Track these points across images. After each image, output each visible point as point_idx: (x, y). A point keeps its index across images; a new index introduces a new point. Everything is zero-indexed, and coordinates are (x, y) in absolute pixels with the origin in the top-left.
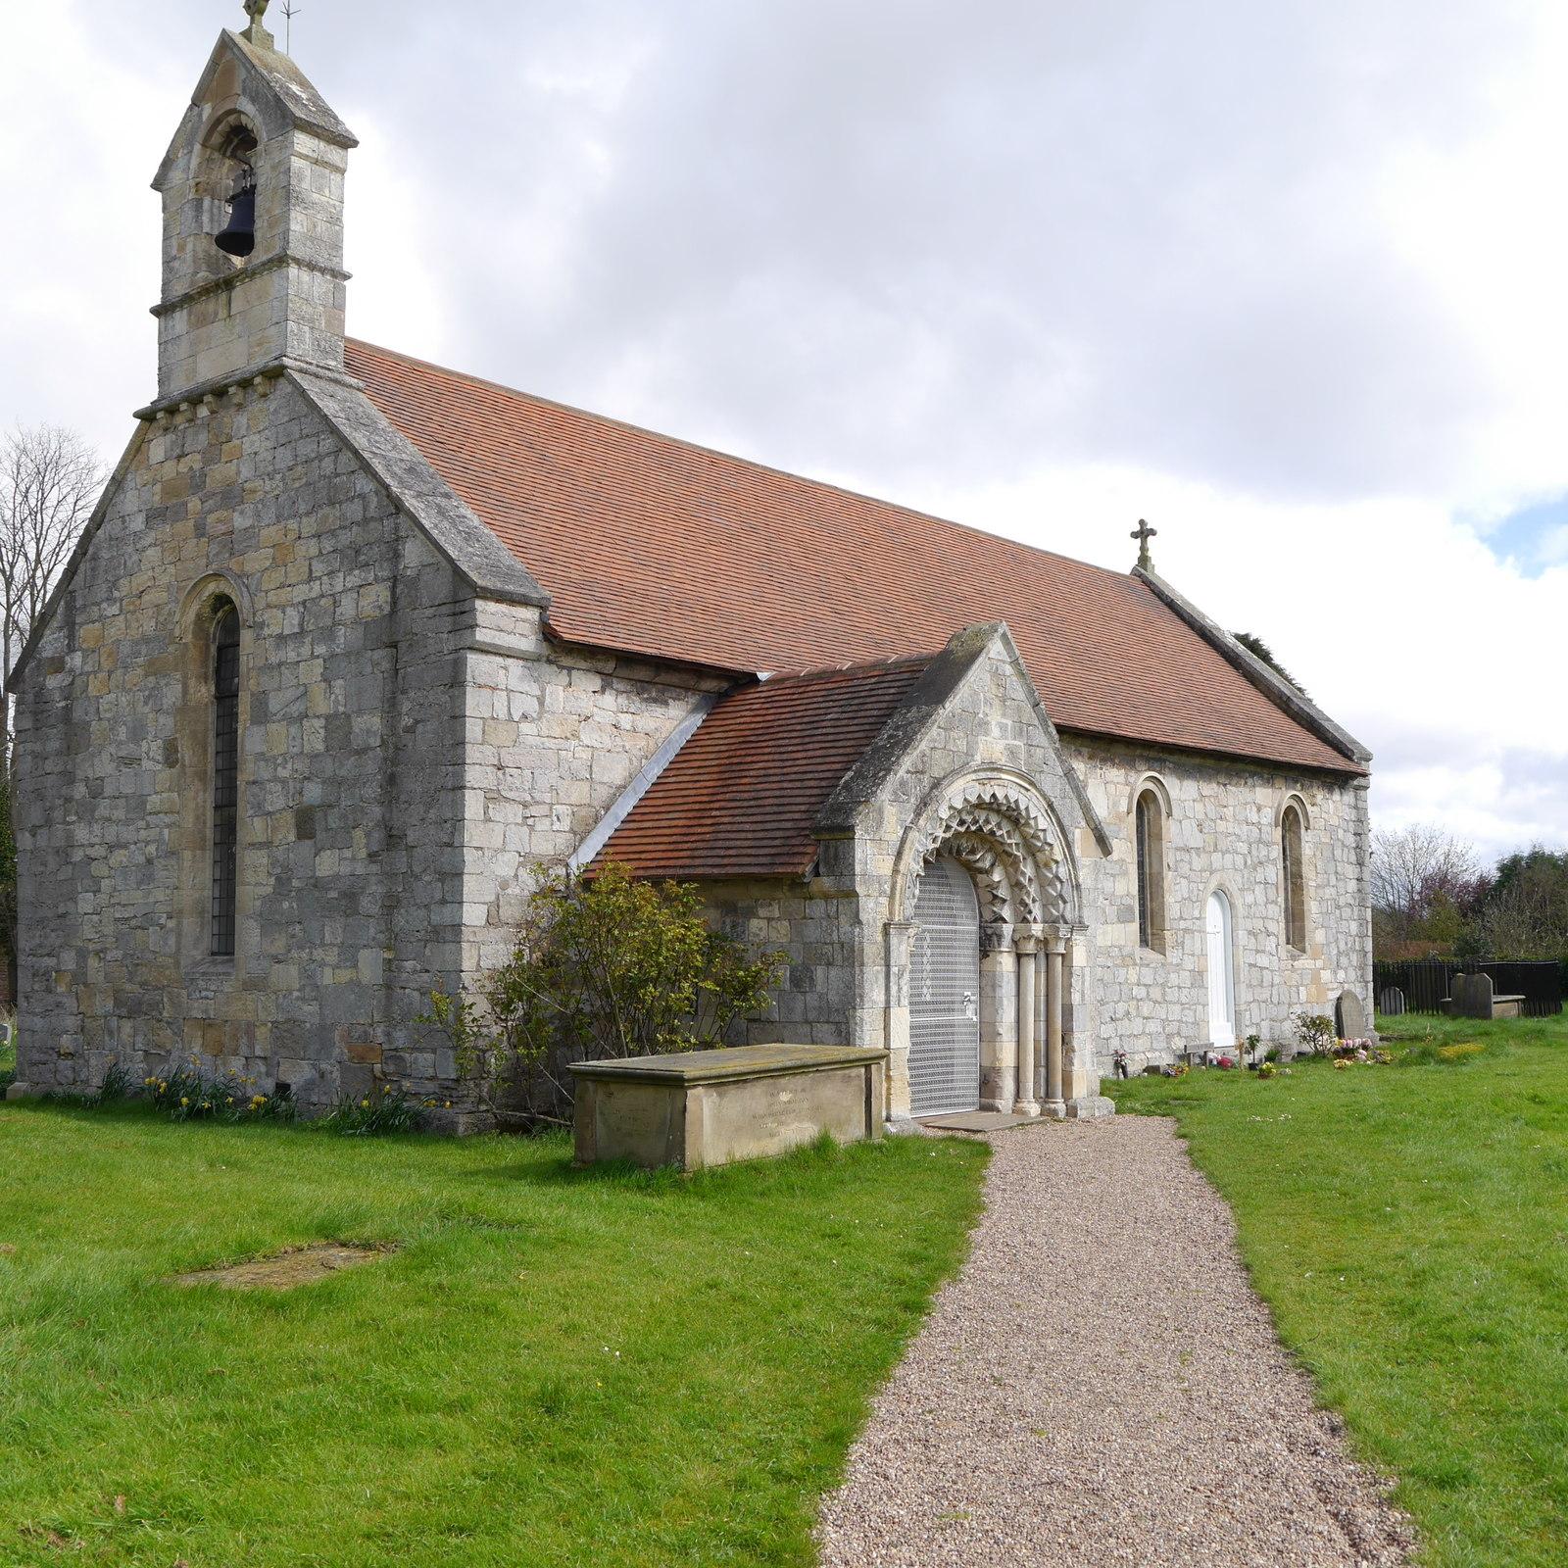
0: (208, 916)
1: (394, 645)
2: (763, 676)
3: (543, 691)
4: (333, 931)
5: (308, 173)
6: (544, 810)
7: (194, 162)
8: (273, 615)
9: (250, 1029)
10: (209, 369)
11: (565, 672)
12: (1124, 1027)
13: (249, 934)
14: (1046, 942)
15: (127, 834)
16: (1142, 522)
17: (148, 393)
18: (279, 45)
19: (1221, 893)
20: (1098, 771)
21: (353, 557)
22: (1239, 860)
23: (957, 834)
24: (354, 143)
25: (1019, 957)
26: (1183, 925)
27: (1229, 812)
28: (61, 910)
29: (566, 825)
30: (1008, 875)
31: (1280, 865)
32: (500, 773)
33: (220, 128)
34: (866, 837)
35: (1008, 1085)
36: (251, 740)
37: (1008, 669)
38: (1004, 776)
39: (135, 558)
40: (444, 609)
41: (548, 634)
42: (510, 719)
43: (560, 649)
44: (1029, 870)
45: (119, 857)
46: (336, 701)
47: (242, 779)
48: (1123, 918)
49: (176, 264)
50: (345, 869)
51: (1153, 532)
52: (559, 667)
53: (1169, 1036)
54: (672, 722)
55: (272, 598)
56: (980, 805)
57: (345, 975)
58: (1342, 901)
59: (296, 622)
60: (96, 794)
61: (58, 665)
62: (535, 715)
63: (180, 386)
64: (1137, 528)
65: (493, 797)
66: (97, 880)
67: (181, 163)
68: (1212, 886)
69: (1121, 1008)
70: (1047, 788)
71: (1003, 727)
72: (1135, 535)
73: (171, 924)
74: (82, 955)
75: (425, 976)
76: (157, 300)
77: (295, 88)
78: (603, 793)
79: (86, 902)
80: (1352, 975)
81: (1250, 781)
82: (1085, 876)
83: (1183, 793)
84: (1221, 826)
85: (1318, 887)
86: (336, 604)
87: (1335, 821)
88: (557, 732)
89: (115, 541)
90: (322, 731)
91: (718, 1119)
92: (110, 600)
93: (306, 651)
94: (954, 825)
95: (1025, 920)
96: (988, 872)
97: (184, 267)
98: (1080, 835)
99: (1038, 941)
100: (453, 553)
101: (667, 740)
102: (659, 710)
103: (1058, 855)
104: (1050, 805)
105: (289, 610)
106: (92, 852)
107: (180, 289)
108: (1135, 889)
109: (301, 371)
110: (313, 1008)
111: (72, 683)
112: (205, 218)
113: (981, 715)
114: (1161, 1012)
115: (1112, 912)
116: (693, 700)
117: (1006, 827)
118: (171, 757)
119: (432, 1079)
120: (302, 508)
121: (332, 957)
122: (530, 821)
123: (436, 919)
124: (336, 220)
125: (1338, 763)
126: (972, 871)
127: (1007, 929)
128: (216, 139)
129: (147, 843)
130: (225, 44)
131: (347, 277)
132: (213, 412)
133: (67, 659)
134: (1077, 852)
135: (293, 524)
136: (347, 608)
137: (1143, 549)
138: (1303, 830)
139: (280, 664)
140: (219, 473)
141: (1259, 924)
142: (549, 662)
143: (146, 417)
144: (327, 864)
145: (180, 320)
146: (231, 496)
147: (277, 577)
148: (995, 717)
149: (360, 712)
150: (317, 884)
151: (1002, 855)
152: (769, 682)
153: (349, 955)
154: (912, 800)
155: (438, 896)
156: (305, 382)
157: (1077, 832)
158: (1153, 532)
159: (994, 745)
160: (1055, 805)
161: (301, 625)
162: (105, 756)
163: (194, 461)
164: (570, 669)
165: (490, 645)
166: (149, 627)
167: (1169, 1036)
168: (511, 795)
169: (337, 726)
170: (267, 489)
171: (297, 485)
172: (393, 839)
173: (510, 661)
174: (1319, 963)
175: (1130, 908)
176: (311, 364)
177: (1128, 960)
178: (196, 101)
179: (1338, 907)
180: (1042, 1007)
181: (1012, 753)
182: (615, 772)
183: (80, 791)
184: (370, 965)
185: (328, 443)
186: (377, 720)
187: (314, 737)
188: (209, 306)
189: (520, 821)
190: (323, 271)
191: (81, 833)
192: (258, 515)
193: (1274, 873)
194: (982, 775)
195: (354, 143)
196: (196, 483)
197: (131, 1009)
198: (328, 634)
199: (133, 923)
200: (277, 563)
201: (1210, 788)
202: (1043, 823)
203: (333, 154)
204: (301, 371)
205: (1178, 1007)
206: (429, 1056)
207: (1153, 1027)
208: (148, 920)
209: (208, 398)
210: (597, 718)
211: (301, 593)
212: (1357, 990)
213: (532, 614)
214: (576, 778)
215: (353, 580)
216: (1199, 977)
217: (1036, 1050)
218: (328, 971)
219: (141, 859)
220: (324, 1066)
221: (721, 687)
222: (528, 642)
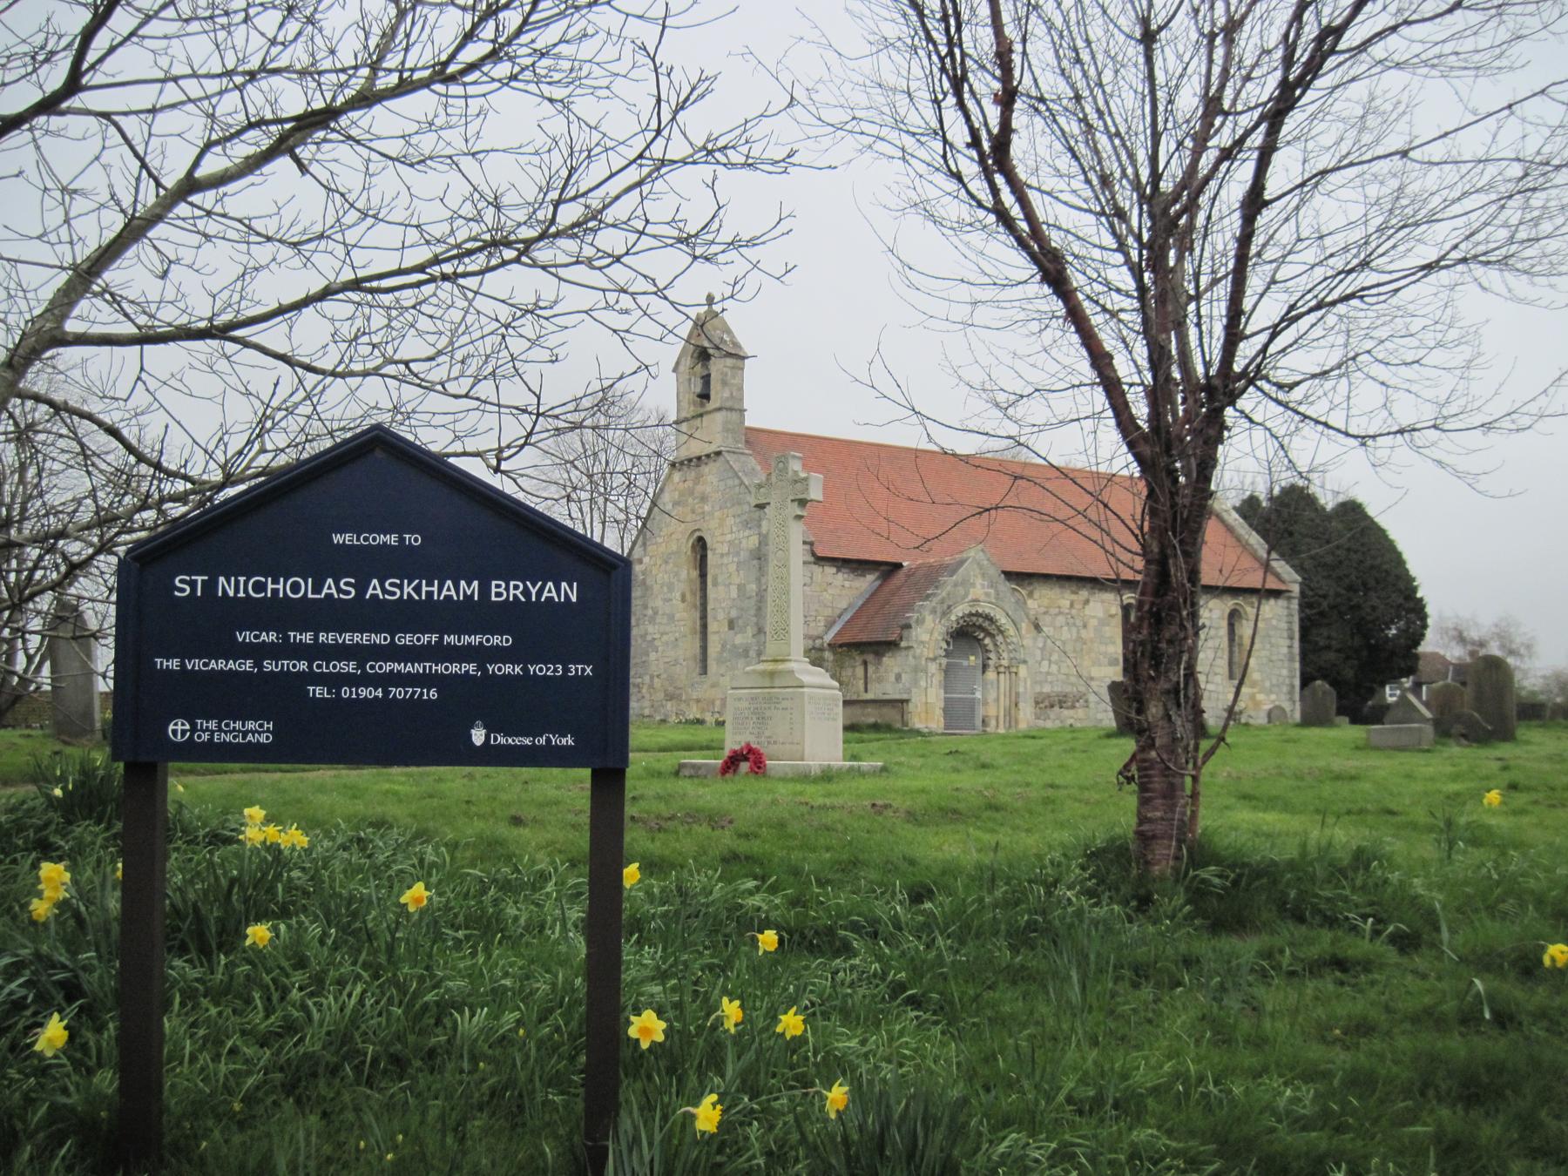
9: (713, 703)
13: (712, 666)
15: (668, 629)
21: (746, 524)
35: (993, 723)
44: (1000, 638)
45: (665, 638)
54: (869, 581)
56: (971, 614)
60: (656, 613)
74: (652, 677)
79: (653, 656)
80: (1283, 697)
82: (1027, 642)
97: (685, 404)
107: (684, 415)
118: (683, 600)
124: (741, 389)
136: (744, 544)
140: (699, 488)
144: (739, 639)
146: (704, 499)
148: (979, 581)
150: (734, 646)
151: (988, 634)
163: (689, 484)
166: (674, 548)
169: (741, 588)
175: (1117, 659)
181: (987, 595)
182: (844, 605)
183: (650, 612)
185: (737, 482)
186: (754, 587)
187: (734, 594)
191: (650, 629)
196: (691, 492)
197: (670, 697)
198: (738, 554)
200: (721, 525)
203: (739, 363)
208: (676, 663)
211: (729, 537)
212: (1287, 706)
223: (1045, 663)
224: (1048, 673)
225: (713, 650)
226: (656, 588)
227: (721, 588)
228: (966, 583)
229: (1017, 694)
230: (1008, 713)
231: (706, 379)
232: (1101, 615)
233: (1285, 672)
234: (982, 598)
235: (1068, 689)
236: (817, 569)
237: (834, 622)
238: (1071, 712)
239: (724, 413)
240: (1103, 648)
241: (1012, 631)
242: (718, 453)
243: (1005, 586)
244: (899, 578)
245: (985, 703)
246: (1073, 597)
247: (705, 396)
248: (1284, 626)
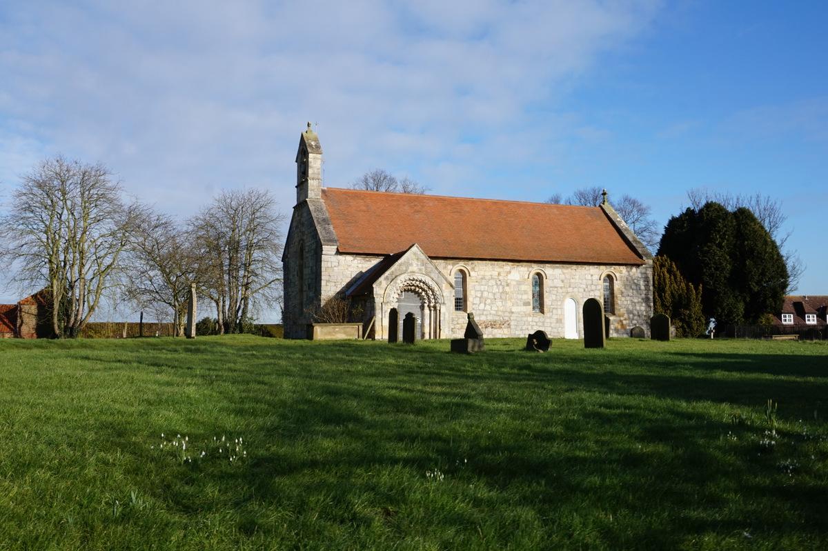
17: (295, 203)
22: (582, 290)
65: (328, 281)
69: (524, 328)
76: (296, 185)
83: (550, 272)
84: (572, 281)
91: (321, 331)
134: (443, 289)
138: (615, 281)
148: (414, 263)
157: (444, 285)
159: (414, 268)
160: (435, 279)
181: (420, 270)
223: (482, 305)
224: (484, 310)
228: (408, 264)
235: (497, 318)
238: (500, 331)
240: (520, 297)
241: (436, 288)
246: (501, 270)
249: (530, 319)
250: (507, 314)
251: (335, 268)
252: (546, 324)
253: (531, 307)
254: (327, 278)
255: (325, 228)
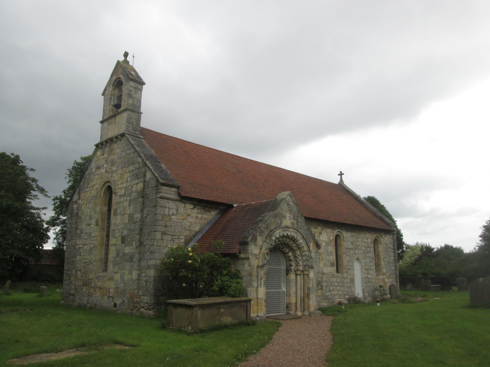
0: (103, 262)
1: (143, 197)
2: (235, 205)
3: (178, 208)
4: (128, 266)
5: (133, 90)
6: (177, 237)
7: (111, 89)
8: (119, 189)
10: (111, 134)
11: (184, 204)
12: (333, 293)
13: (110, 266)
14: (303, 271)
16: (341, 172)
17: (98, 141)
18: (130, 64)
19: (358, 259)
20: (325, 230)
22: (363, 251)
23: (278, 244)
24: (144, 84)
25: (296, 275)
26: (348, 267)
27: (359, 240)
28: (73, 260)
29: (183, 241)
30: (293, 254)
31: (373, 252)
32: (166, 228)
33: (116, 82)
34: (252, 244)
35: (293, 308)
36: (113, 220)
37: (291, 203)
38: (290, 229)
39: (93, 178)
40: (154, 188)
41: (179, 195)
42: (169, 215)
43: (184, 199)
44: (298, 252)
45: (86, 247)
46: (131, 211)
47: (111, 229)
48: (332, 265)
49: (106, 112)
50: (131, 251)
51: (343, 174)
52: (182, 202)
53: (345, 295)
54: (211, 216)
55: (119, 186)
57: (130, 277)
58: (390, 262)
59: (124, 192)
60: (82, 232)
61: (76, 202)
62: (176, 214)
63: (105, 138)
64: (339, 173)
65: (164, 233)
66: (80, 253)
67: (108, 89)
68: (356, 257)
69: (332, 288)
70: (302, 233)
71: (290, 217)
72: (339, 175)
73: (95, 264)
75: (146, 278)
76: (101, 119)
77: (133, 73)
78: (193, 233)
79: (78, 258)
80: (394, 280)
81: (365, 232)
82: (313, 255)
83: (347, 235)
84: (358, 243)
85: (384, 258)
86: (132, 188)
87: (387, 242)
88: (181, 218)
89: (89, 174)
90: (128, 218)
92: (87, 187)
93: (125, 199)
94: (277, 241)
95: (297, 266)
96: (288, 253)
97: (107, 112)
98: (311, 245)
99: (301, 271)
100: (156, 175)
101: (211, 221)
102: (208, 213)
103: (305, 248)
104: (303, 237)
105: (123, 190)
106: (80, 246)
107: (106, 117)
108: (335, 259)
109: (128, 134)
110: (122, 285)
111: (79, 207)
112: (112, 101)
113: (284, 214)
114: (342, 289)
115: (329, 264)
116: (217, 211)
117: (291, 242)
118: (97, 225)
119: (147, 303)
120: (127, 165)
121: (127, 273)
122: (173, 240)
123: (149, 263)
124: (139, 101)
125: (388, 228)
126: (284, 253)
127: (293, 268)
128: (115, 84)
129: (91, 244)
130: (118, 63)
131: (142, 113)
132: (110, 144)
133: (78, 201)
134: (311, 248)
135: (124, 169)
137: (341, 178)
138: (379, 244)
139: (120, 202)
141: (368, 267)
142: (180, 201)
143: (97, 146)
144: (127, 250)
145: (106, 124)
146: (113, 163)
147: (120, 181)
148: (288, 215)
149: (136, 212)
150: (125, 254)
151: (291, 249)
152: (236, 207)
153: (130, 273)
154: (265, 235)
155: (150, 258)
156: (130, 138)
158: (343, 174)
159: (287, 222)
161: (125, 193)
162: (84, 224)
164: (185, 203)
165: (164, 197)
167: (345, 295)
168: (169, 233)
169: (131, 216)
170: (120, 161)
171: (126, 160)
172: (141, 243)
173: (169, 201)
174: (384, 277)
176: (131, 133)
177: (333, 276)
178: (112, 76)
179: (389, 263)
180: (302, 288)
181: (293, 224)
182: (197, 229)
183: (79, 232)
184: (135, 274)
188: (113, 120)
189: (171, 239)
190: (136, 112)
191: (78, 242)
192: (117, 167)
193: (372, 254)
194: (284, 229)
195: (144, 84)
197: (85, 285)
198: (130, 195)
199: (87, 263)
201: (354, 234)
202: (301, 241)
203: (139, 86)
204: (128, 134)
205: (346, 288)
206: (146, 297)
207: (340, 293)
209: (109, 141)
210: (192, 215)
212: (395, 284)
213: (175, 190)
214: (185, 229)
215: (136, 182)
216: (352, 281)
217: (301, 299)
218: (126, 276)
219: (90, 248)
220: (124, 299)
221: (225, 208)
222: (174, 196)
225: (111, 256)
226: (83, 217)
227: (119, 217)
229: (309, 289)
230: (303, 301)
231: (120, 98)
232: (326, 240)
233: (393, 268)
234: (290, 225)
236: (181, 206)
237: (191, 240)
239: (128, 112)
240: (328, 257)
242: (123, 135)
243: (301, 220)
244: (230, 214)
245: (288, 295)
247: (118, 106)
248: (392, 247)
249: (335, 280)
250: (320, 275)
251: (173, 217)
252: (345, 285)
253: (335, 268)
254: (163, 229)
255: (157, 166)
